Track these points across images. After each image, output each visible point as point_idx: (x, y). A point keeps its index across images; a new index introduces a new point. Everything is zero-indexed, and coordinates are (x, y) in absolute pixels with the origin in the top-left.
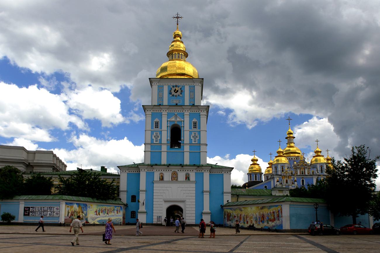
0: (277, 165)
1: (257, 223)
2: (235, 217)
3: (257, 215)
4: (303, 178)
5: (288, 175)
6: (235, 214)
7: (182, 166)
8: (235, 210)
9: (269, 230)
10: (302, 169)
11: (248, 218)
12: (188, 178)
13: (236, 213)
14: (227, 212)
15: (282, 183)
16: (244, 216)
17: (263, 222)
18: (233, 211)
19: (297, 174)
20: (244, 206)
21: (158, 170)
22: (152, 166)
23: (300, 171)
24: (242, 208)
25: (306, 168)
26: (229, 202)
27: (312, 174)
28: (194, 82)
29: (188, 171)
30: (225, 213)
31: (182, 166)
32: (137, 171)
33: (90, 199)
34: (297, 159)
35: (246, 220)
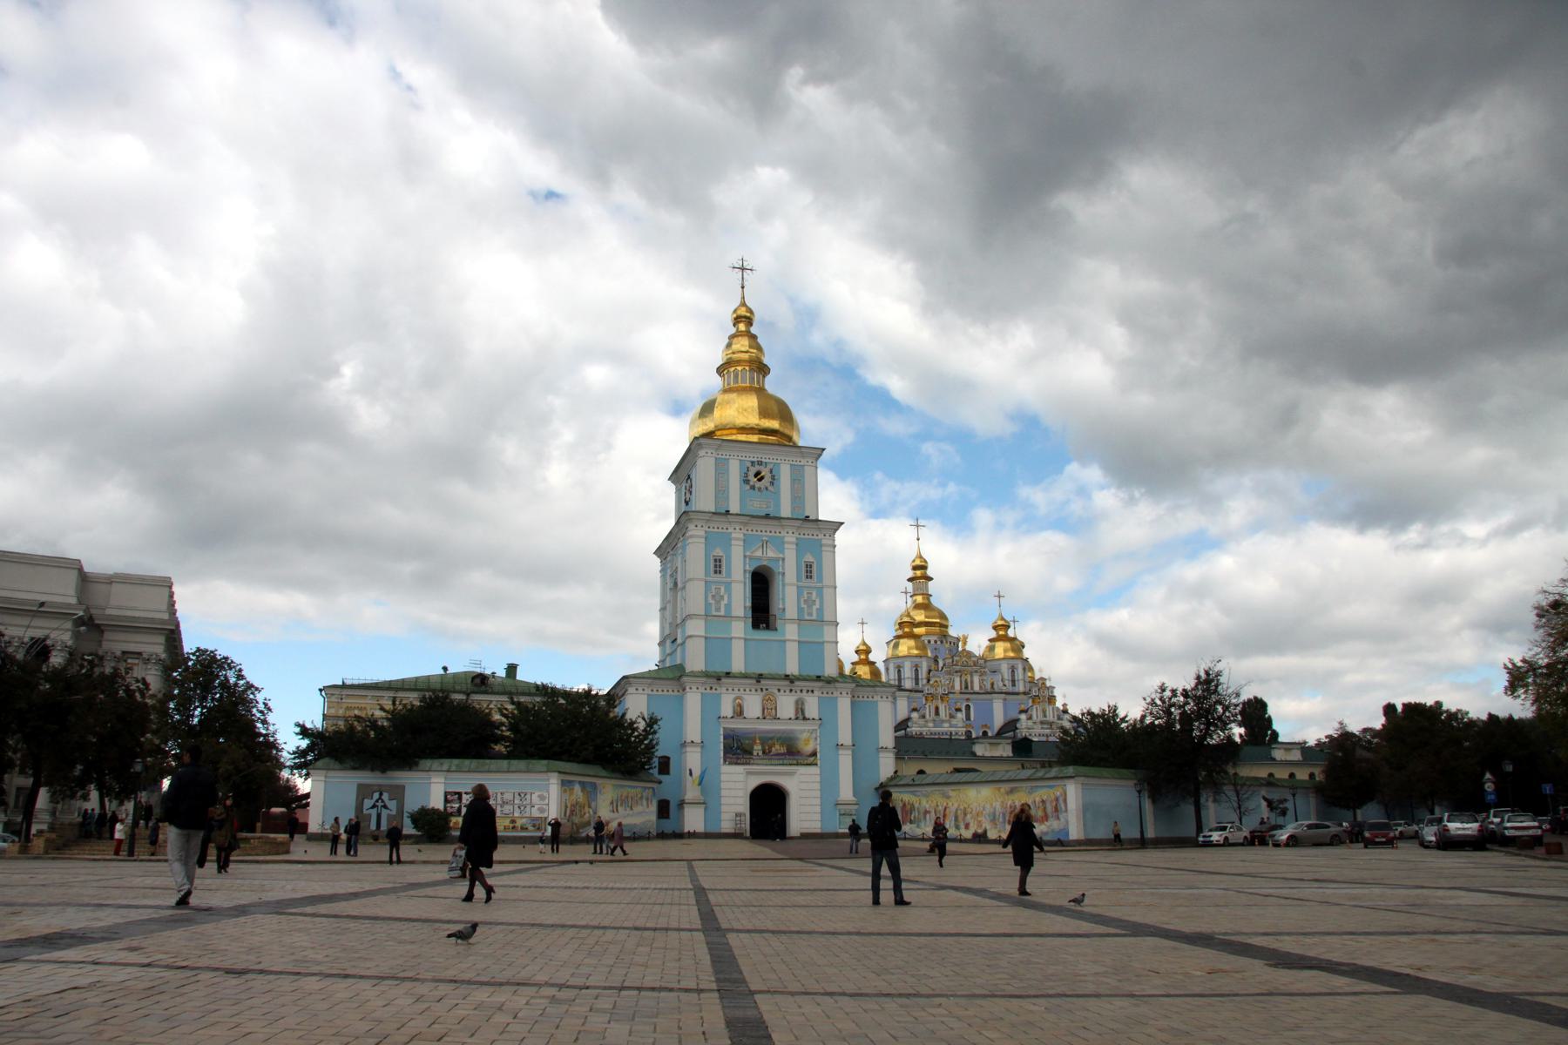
1: (996, 828)
2: (926, 812)
3: (995, 809)
4: (968, 700)
5: (940, 691)
7: (792, 682)
8: (925, 796)
11: (969, 816)
12: (800, 714)
14: (902, 801)
15: (925, 714)
16: (957, 810)
19: (953, 687)
20: (953, 787)
21: (730, 689)
22: (719, 679)
23: (961, 681)
25: (976, 672)
26: (898, 774)
28: (803, 457)
31: (792, 682)
32: (673, 691)
33: (598, 770)
34: (942, 642)
35: (964, 820)
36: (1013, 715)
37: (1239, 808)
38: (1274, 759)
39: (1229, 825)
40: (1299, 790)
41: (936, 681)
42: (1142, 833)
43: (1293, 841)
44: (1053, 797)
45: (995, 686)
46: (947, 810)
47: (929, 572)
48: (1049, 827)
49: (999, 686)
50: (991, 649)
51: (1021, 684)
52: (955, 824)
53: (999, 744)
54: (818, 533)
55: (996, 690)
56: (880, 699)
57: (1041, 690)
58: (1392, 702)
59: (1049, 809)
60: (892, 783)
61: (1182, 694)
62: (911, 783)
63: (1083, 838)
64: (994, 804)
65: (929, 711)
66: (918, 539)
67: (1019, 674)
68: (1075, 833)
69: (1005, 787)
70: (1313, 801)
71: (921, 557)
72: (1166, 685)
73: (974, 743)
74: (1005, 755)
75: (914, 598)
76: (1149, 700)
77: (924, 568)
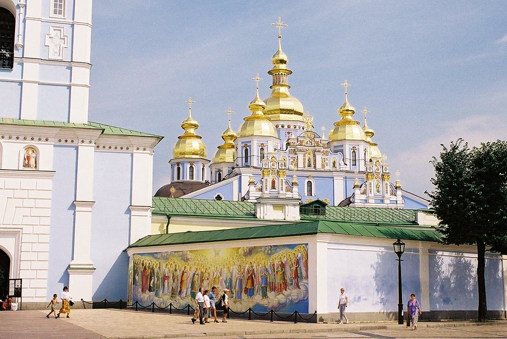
0: (250, 142)
2: (165, 278)
3: (232, 274)
6: (167, 270)
11: (205, 283)
14: (143, 264)
17: (250, 292)
18: (162, 261)
23: (304, 160)
24: (188, 253)
29: (32, 142)
30: (134, 266)
44: (293, 261)
46: (185, 274)
48: (287, 297)
51: (362, 163)
52: (191, 292)
55: (338, 169)
59: (289, 274)
64: (232, 268)
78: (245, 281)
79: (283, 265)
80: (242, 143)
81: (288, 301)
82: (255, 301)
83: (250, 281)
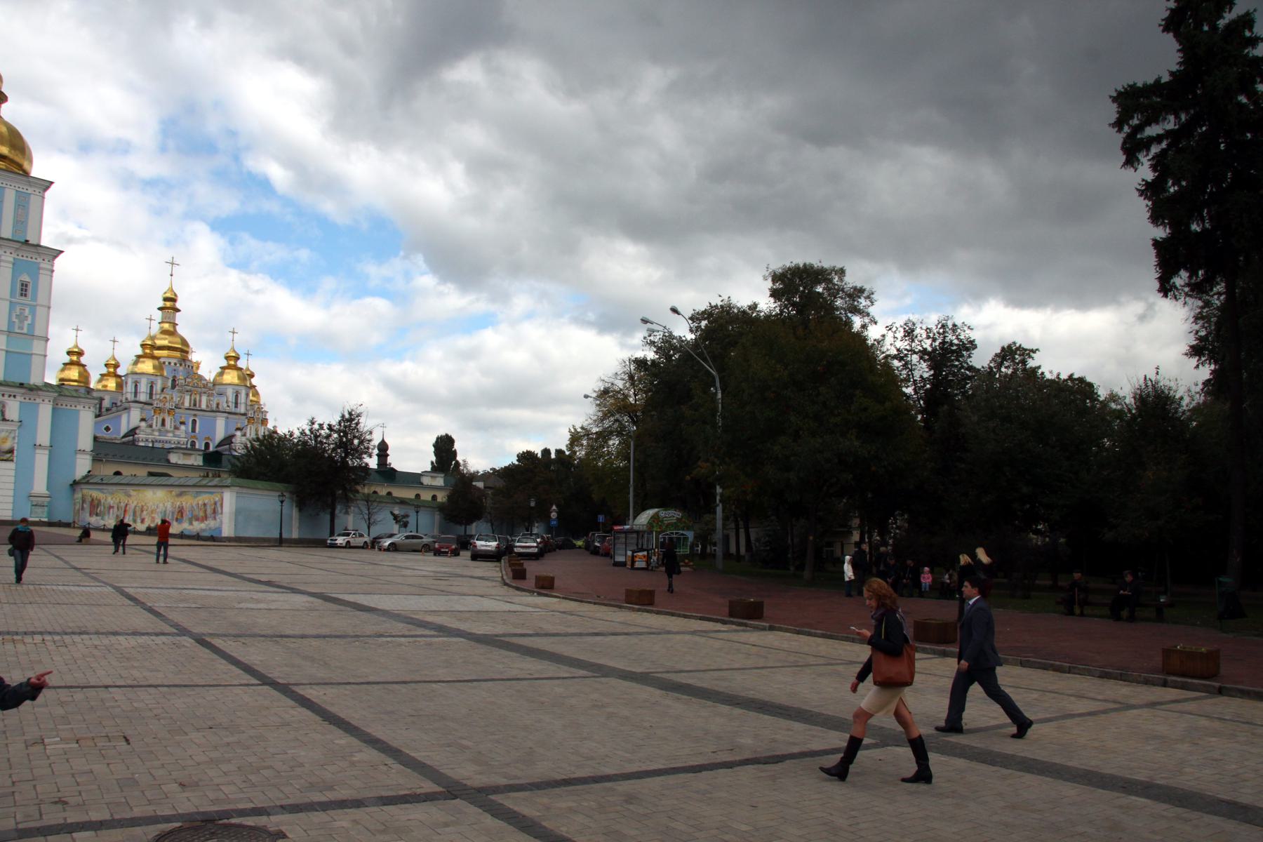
2: (111, 507)
3: (166, 508)
4: (195, 415)
5: (168, 406)
6: (112, 502)
8: (113, 494)
9: (197, 537)
10: (196, 394)
11: (145, 513)
13: (114, 499)
14: (91, 496)
16: (136, 506)
18: (107, 495)
19: (183, 403)
25: (205, 393)
27: (214, 409)
34: (181, 365)
35: (141, 515)
36: (232, 431)
37: (369, 519)
38: (422, 484)
39: (353, 532)
40: (422, 508)
41: (165, 398)
42: (281, 534)
43: (394, 548)
44: (213, 502)
45: (220, 407)
47: (178, 305)
48: (207, 525)
49: (223, 406)
50: (221, 374)
53: (191, 454)
54: (37, 257)
55: (221, 409)
56: (82, 408)
57: (256, 414)
58: (548, 448)
59: (209, 511)
60: (84, 481)
61: (328, 429)
62: (99, 482)
63: (233, 536)
64: (166, 504)
65: (156, 422)
66: (171, 275)
67: (242, 398)
68: (227, 531)
69: (176, 491)
70: (437, 517)
71: (172, 290)
72: (315, 420)
73: (169, 452)
74: (195, 464)
75: (162, 325)
76: (301, 430)
77: (174, 300)
78: (176, 513)
79: (205, 505)
80: (132, 379)
81: (208, 528)
82: (184, 527)
83: (180, 514)
